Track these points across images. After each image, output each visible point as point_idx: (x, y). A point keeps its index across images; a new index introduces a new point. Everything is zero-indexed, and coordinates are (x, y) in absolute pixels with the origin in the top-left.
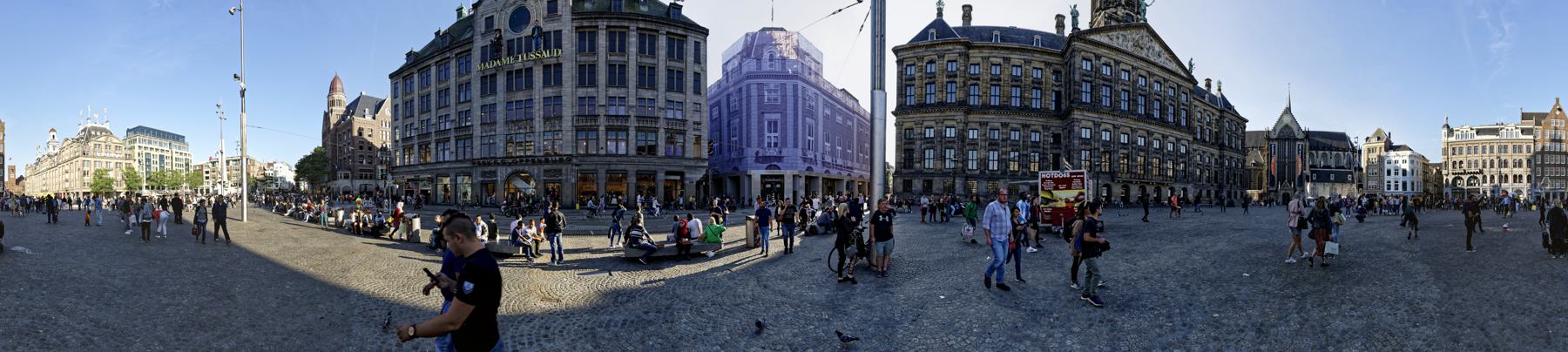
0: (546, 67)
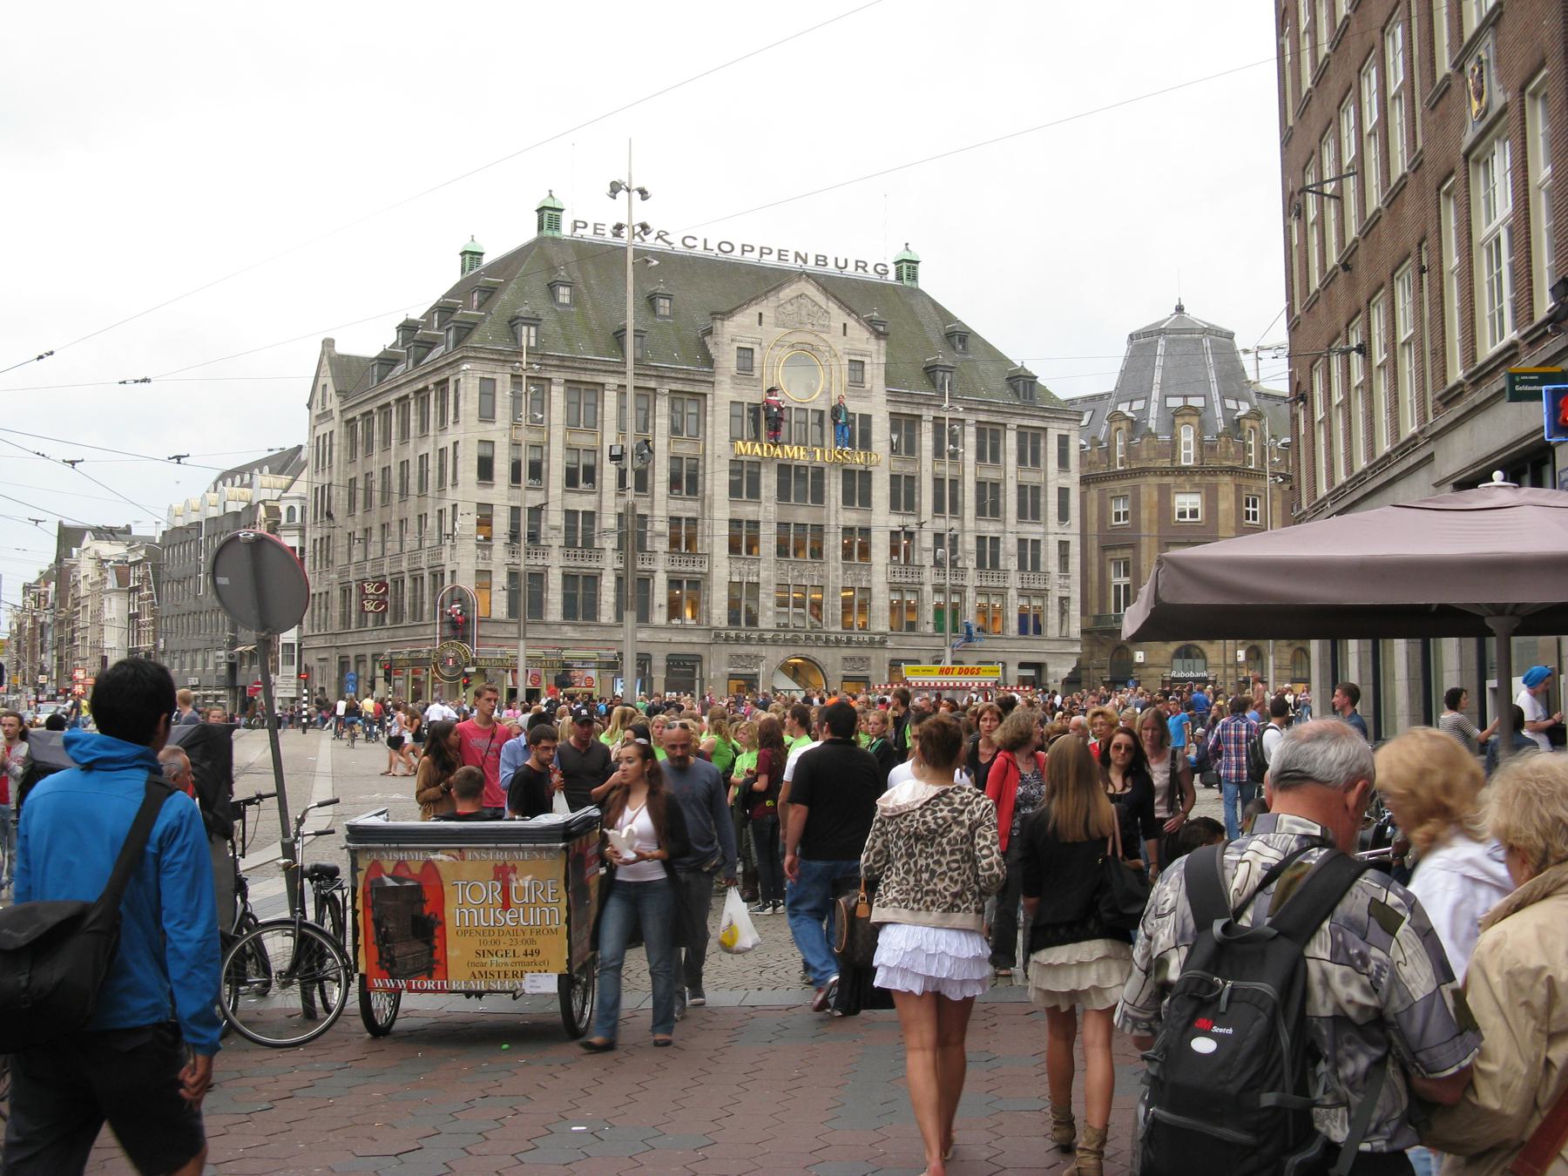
0: (848, 475)
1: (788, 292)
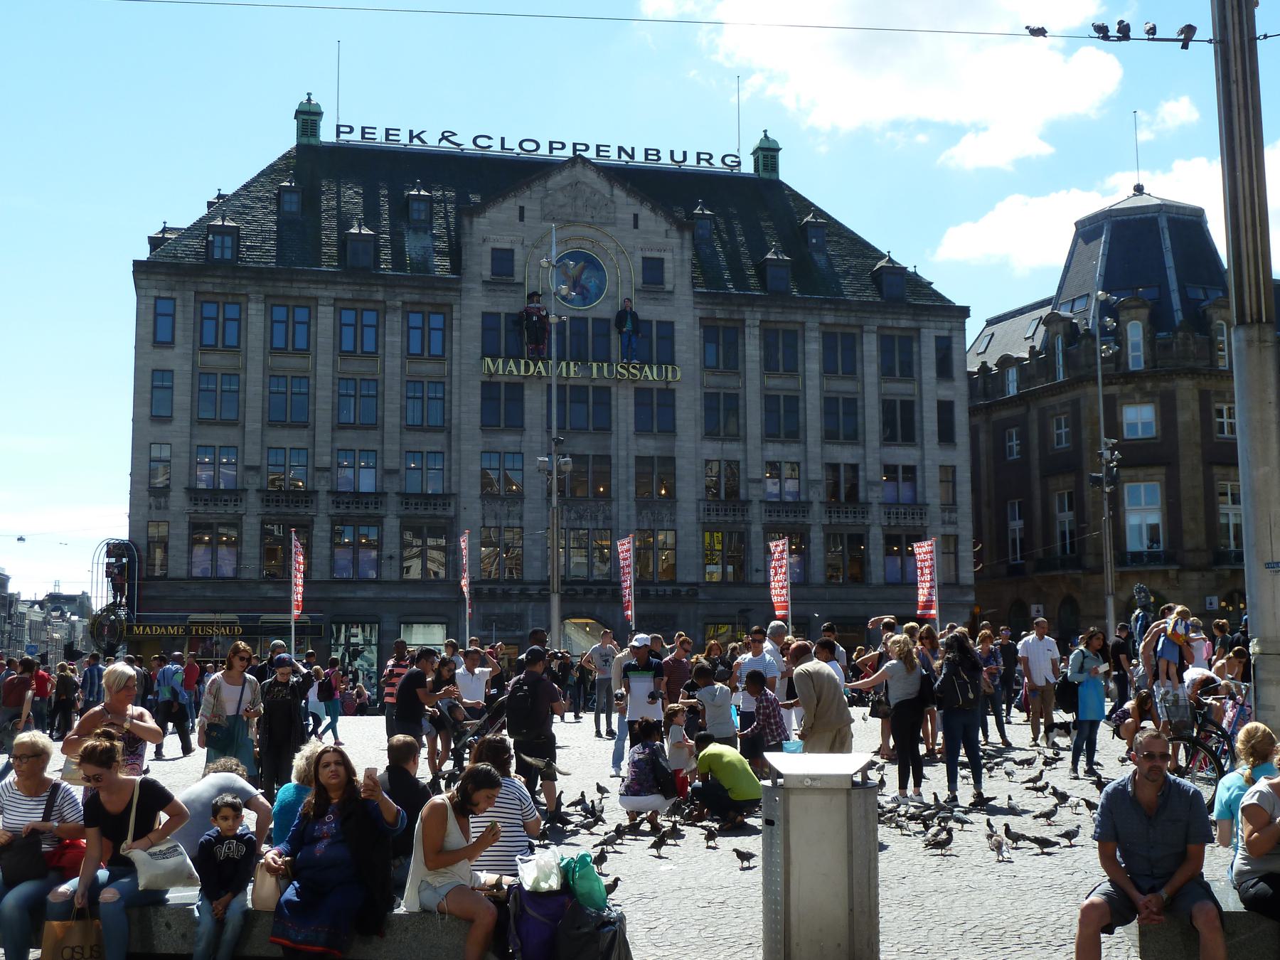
0: (643, 395)
1: (557, 180)
